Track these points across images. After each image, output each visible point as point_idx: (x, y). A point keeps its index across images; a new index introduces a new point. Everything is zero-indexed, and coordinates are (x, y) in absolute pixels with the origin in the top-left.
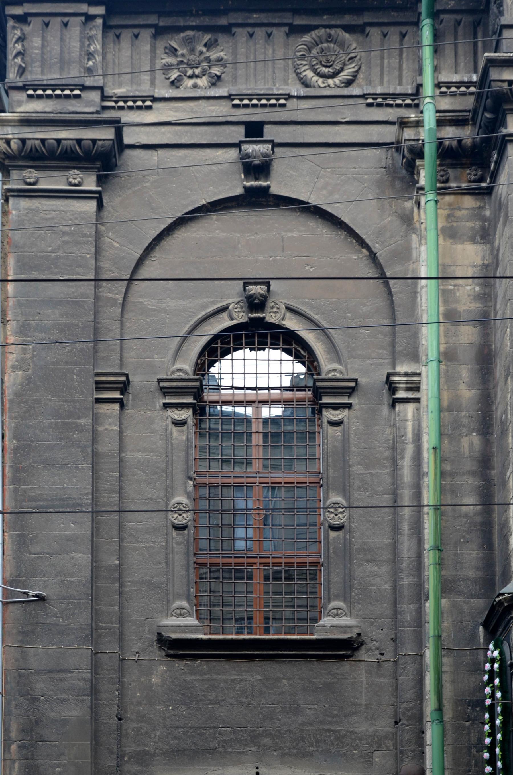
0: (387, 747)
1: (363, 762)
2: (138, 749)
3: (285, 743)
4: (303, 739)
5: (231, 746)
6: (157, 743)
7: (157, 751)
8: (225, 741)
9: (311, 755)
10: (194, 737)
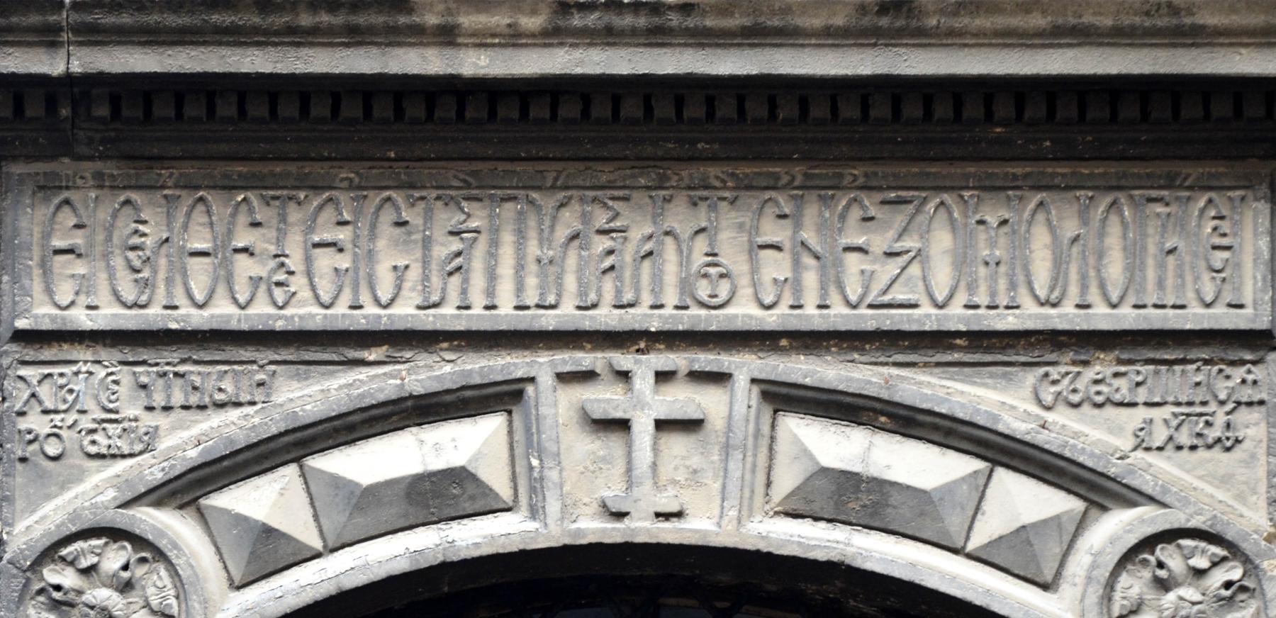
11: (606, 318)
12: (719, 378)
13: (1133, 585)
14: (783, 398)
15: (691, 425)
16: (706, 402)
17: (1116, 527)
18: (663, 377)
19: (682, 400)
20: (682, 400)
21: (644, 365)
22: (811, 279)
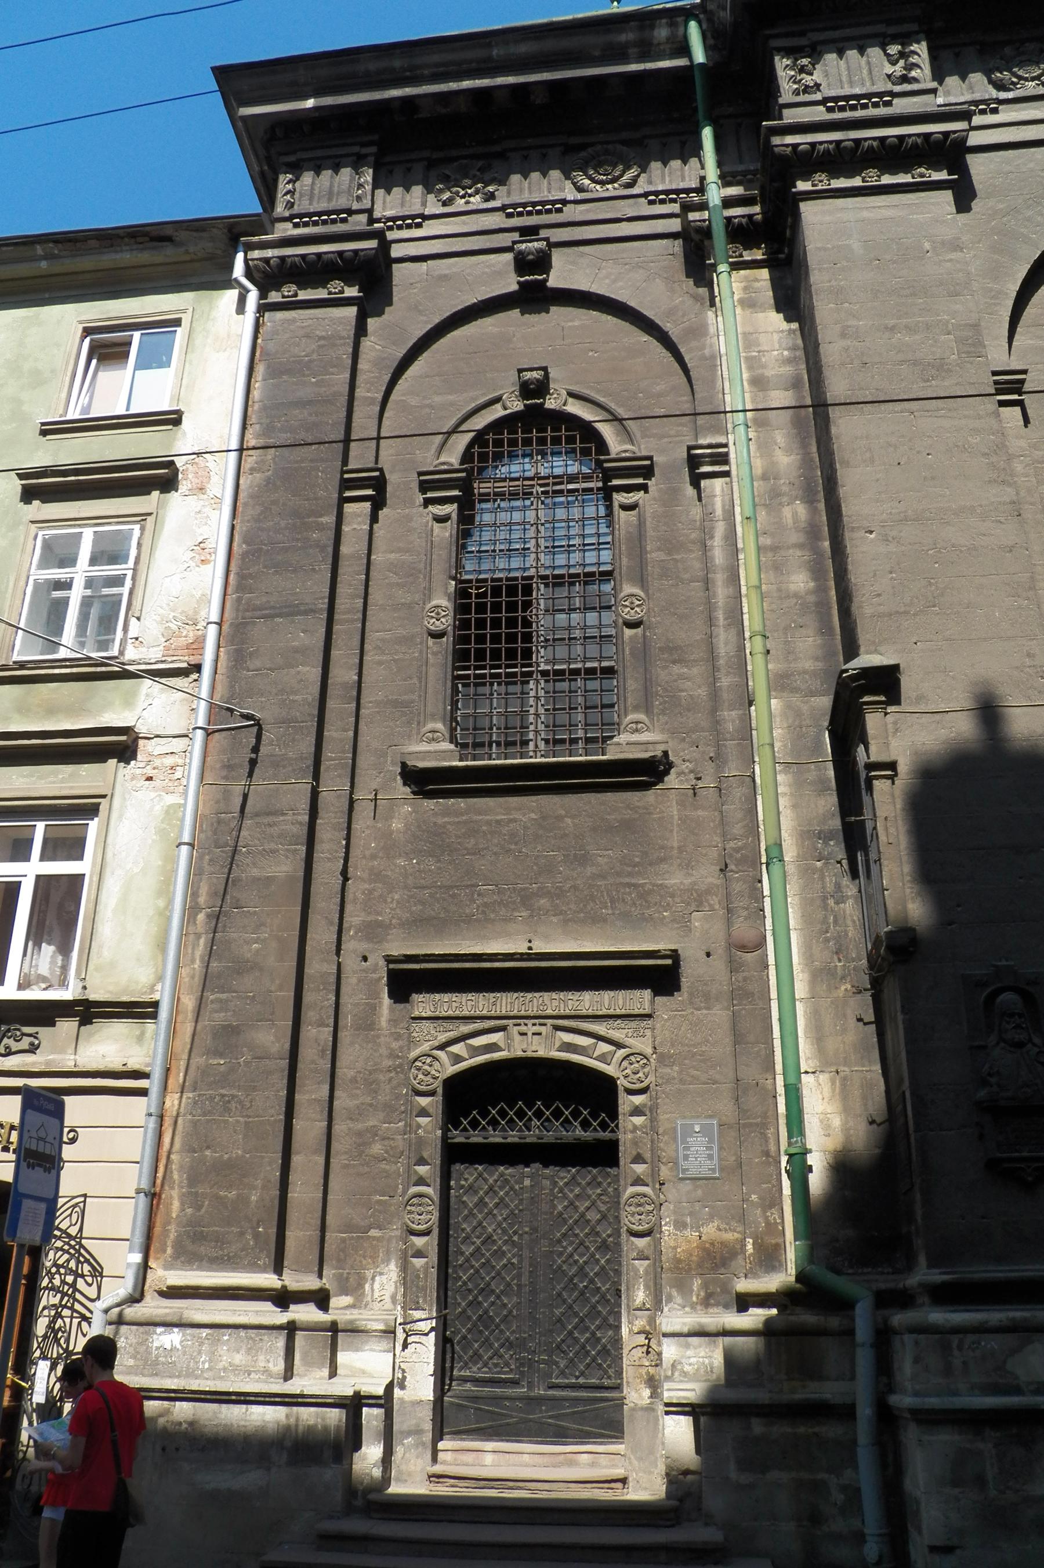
0: (710, 905)
1: (678, 928)
2: (369, 919)
3: (568, 904)
4: (593, 898)
5: (493, 911)
6: (394, 909)
7: (394, 921)
8: (486, 905)
9: (605, 921)
10: (444, 900)
11: (523, 1013)
12: (545, 1025)
13: (625, 1063)
14: (557, 1028)
15: (540, 1034)
16: (543, 1029)
17: (622, 1053)
18: (534, 1025)
19: (536, 1029)
20: (536, 1029)
21: (530, 1022)
22: (562, 1006)
